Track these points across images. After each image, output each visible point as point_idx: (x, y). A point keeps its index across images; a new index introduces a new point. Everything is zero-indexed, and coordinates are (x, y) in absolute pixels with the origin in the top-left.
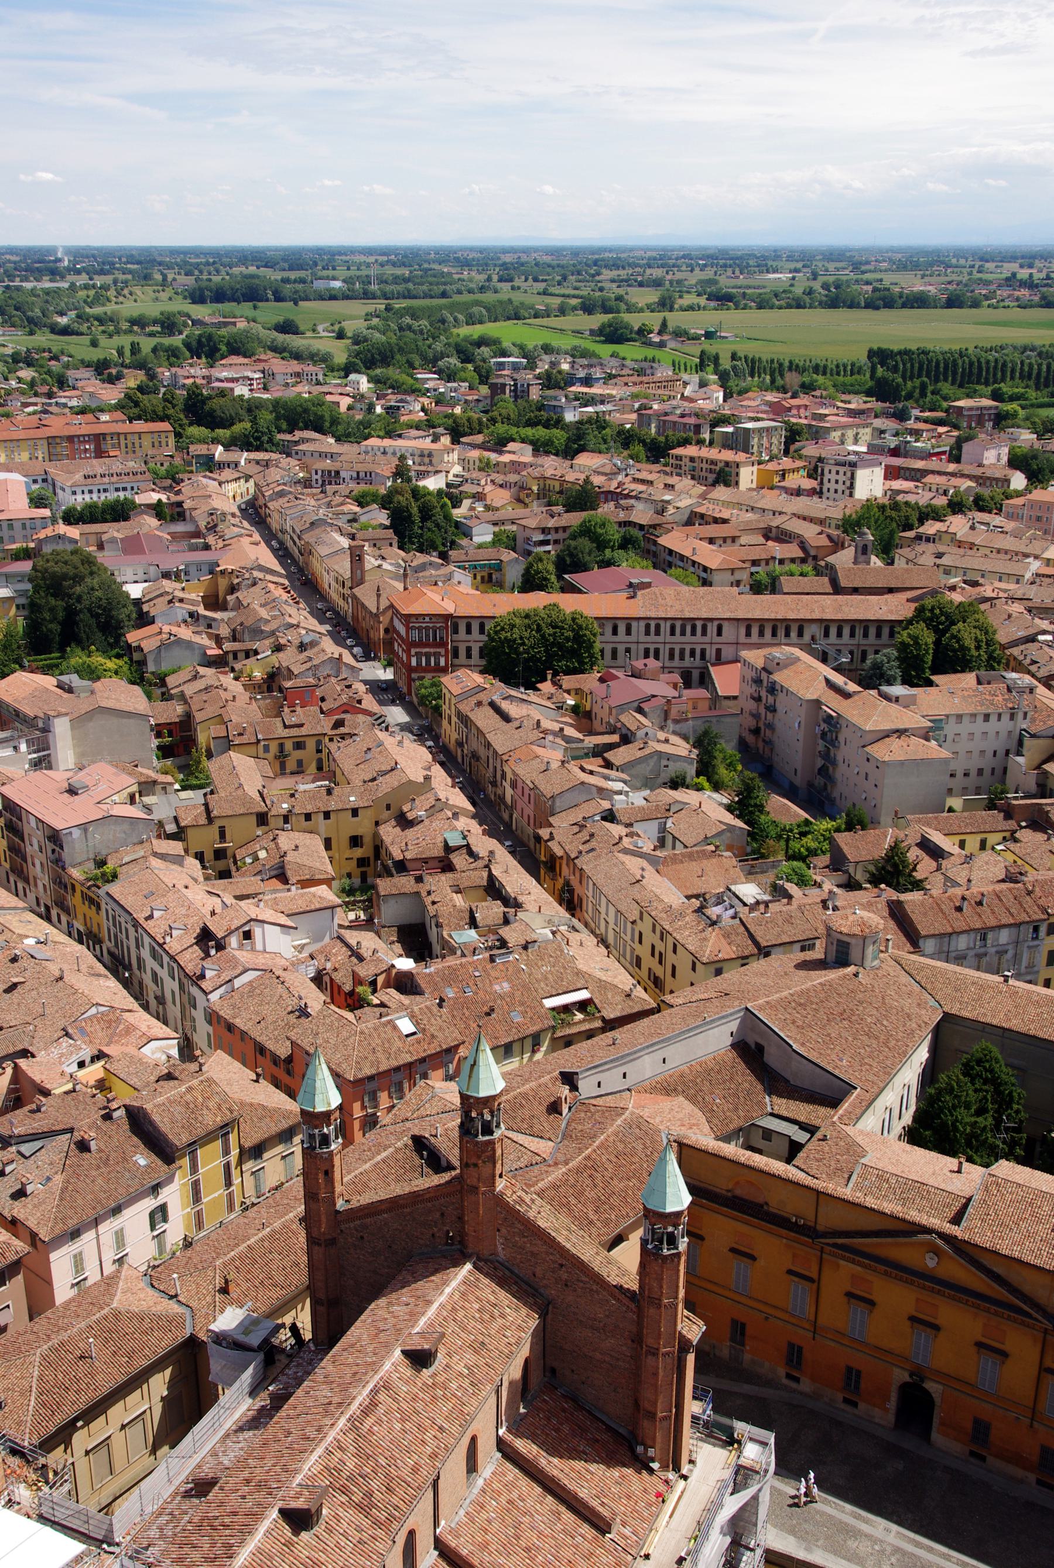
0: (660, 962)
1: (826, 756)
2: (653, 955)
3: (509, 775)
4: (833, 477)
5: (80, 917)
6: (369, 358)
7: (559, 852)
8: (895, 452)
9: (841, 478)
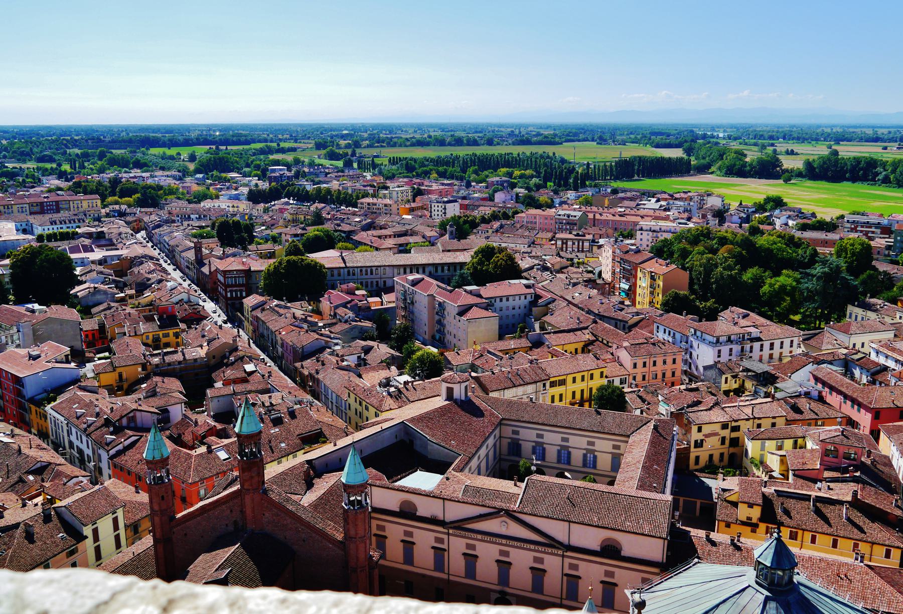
1: (439, 322)
3: (280, 342)
4: (436, 208)
5: (35, 426)
6: (205, 168)
7: (306, 372)
8: (464, 198)
9: (440, 209)
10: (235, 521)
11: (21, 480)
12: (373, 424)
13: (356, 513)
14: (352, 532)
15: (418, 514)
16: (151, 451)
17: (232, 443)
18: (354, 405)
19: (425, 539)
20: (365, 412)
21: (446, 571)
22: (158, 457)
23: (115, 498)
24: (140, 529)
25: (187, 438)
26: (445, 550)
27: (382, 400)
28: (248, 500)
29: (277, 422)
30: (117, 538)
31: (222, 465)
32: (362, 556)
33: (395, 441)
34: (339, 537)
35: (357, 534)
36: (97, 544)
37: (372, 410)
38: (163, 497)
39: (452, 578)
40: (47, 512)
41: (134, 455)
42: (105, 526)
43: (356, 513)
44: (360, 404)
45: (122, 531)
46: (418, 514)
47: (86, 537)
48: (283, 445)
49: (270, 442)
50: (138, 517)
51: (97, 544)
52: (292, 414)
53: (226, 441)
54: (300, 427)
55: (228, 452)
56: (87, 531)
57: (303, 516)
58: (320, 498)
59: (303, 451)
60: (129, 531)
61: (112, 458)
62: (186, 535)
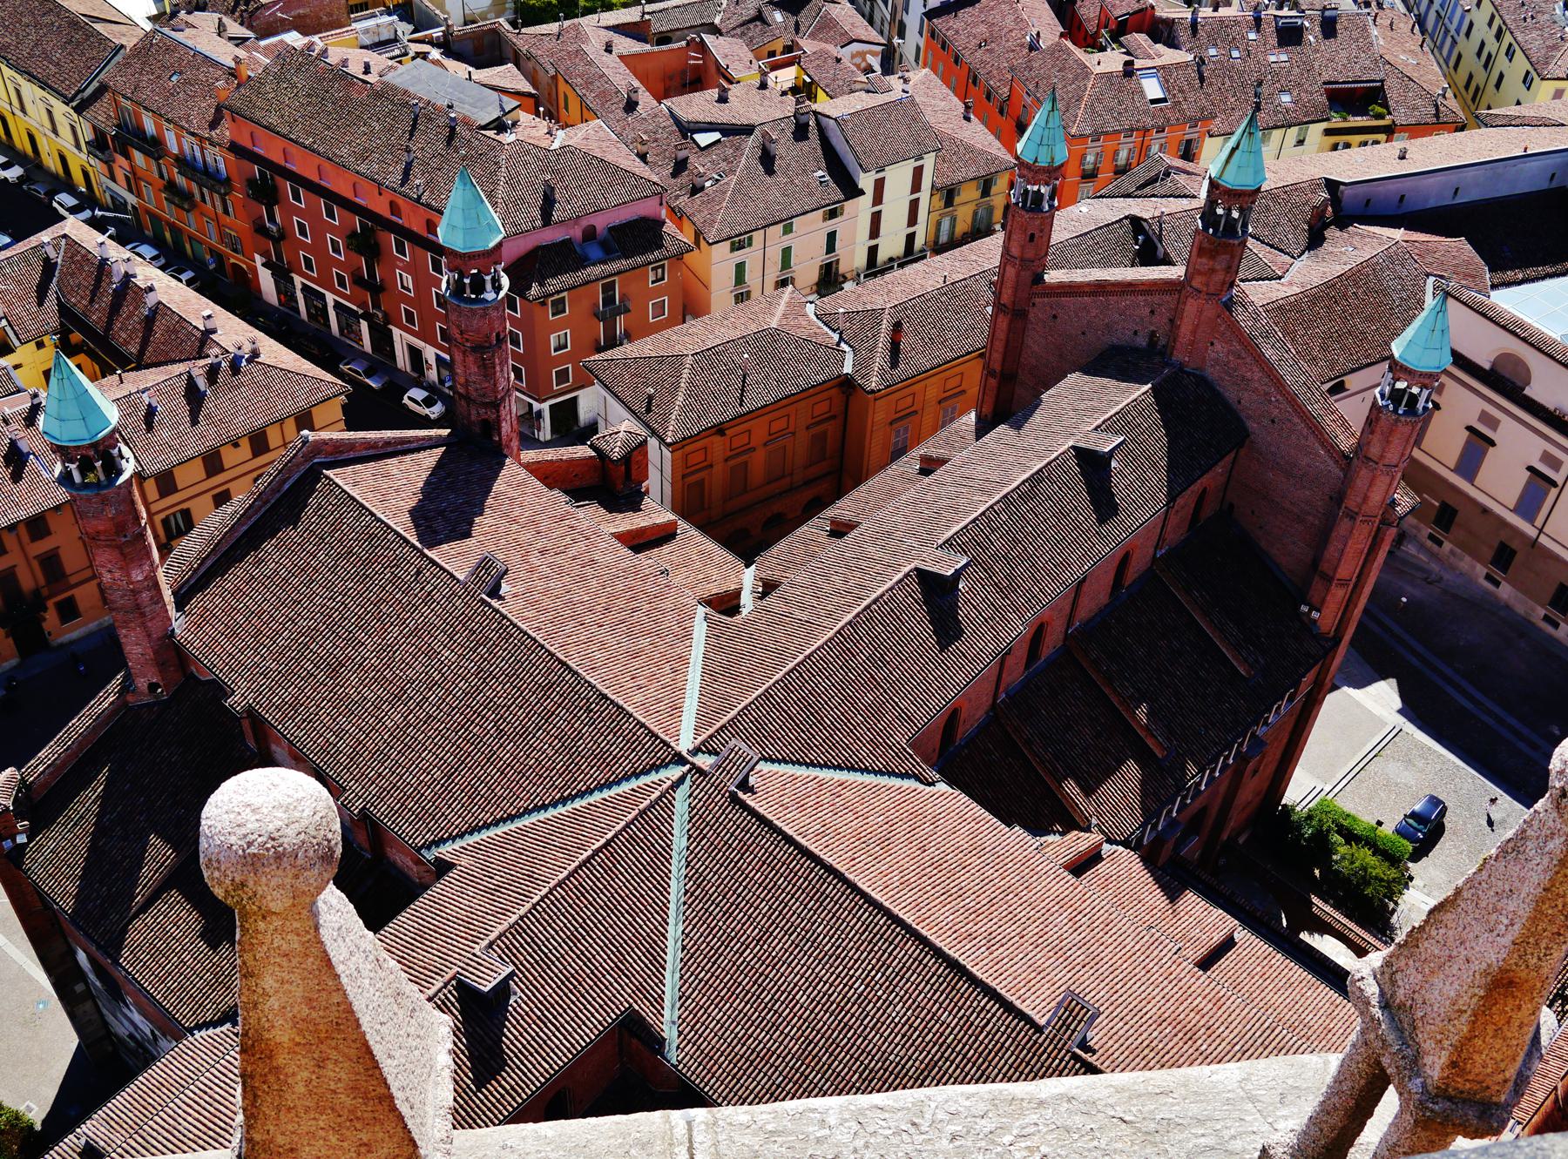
0: (1486, 66)
2: (1479, 54)
10: (1153, 334)
11: (759, 17)
12: (1509, 122)
13: (1397, 421)
14: (1374, 451)
15: (1527, 391)
16: (1033, 146)
17: (1178, 66)
18: (1482, 32)
19: (1518, 446)
20: (1502, 58)
21: (1539, 523)
22: (1043, 163)
23: (927, 127)
24: (957, 200)
25: (1088, 11)
26: (1554, 484)
27: (1555, 47)
28: (1191, 307)
29: (1290, 36)
30: (914, 205)
31: (1145, 112)
32: (1376, 497)
33: (1545, 185)
34: (1345, 443)
35: (1382, 457)
36: (877, 209)
37: (1521, 64)
38: (1032, 237)
39: (1543, 540)
40: (803, 119)
41: (975, 25)
42: (898, 178)
43: (1397, 421)
44: (1499, 35)
45: (924, 196)
46: (1527, 391)
47: (862, 193)
48: (1286, 98)
49: (1260, 84)
50: (959, 176)
51: (877, 209)
52: (1329, 27)
53: (1169, 56)
54: (1336, 62)
55: (1165, 84)
56: (866, 181)
57: (1289, 379)
58: (1330, 285)
59: (1324, 125)
60: (936, 197)
61: (931, 14)
62: (1055, 317)
